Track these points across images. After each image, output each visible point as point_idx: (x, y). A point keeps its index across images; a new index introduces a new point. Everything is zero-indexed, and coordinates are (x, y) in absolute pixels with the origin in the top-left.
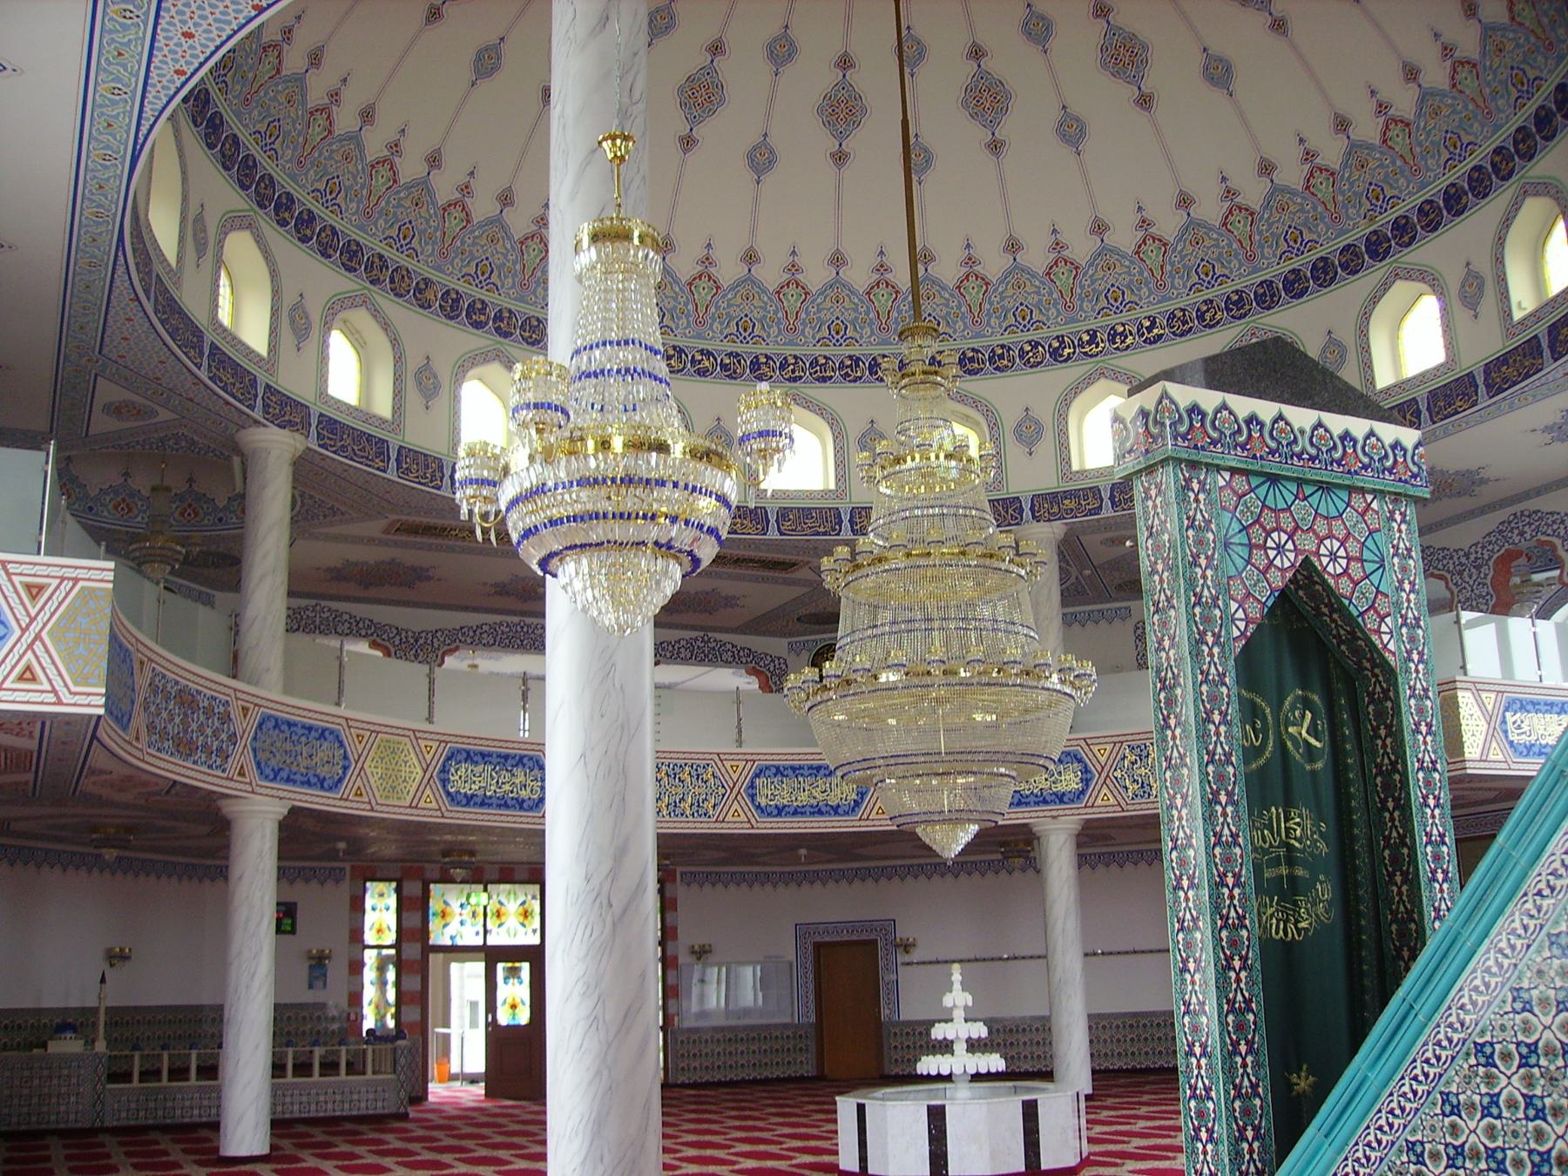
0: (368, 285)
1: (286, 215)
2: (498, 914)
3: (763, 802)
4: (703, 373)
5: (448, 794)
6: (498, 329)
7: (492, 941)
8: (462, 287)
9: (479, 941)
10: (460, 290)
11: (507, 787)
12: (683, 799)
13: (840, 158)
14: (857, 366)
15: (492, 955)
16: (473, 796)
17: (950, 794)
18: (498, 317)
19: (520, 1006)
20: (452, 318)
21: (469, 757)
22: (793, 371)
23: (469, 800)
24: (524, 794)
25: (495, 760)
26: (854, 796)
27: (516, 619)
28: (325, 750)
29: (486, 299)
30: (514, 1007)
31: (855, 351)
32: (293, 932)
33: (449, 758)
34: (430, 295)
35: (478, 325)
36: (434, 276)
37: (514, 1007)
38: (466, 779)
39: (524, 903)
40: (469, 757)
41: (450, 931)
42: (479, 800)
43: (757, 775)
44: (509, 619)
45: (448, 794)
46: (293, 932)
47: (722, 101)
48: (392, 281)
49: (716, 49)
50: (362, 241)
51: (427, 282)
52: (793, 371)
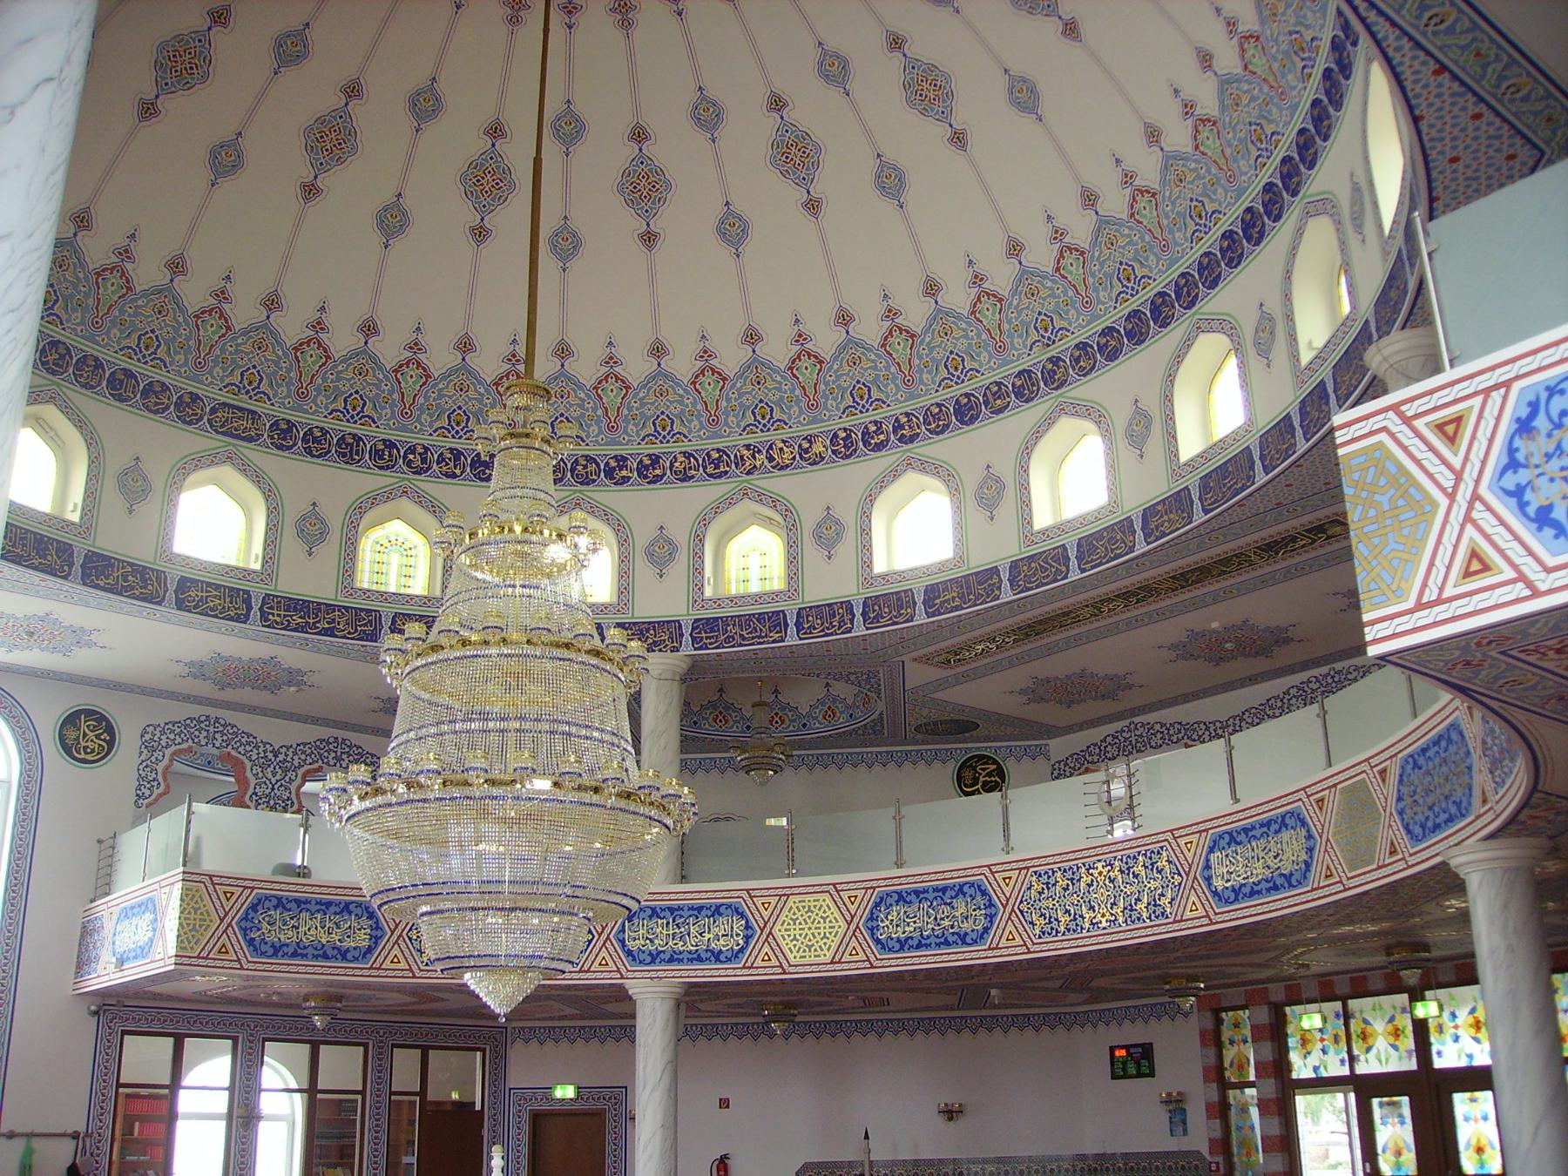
0: (746, 477)
1: (624, 473)
2: (1364, 1036)
3: (1218, 883)
4: (1113, 356)
5: (878, 941)
6: (902, 439)
7: (1361, 1069)
8: (847, 422)
9: (1345, 1071)
10: (846, 425)
11: (946, 923)
12: (1138, 900)
13: (1071, 29)
14: (1234, 241)
15: (1367, 1088)
16: (907, 939)
17: (501, 935)
18: (898, 426)
19: (1488, 1151)
20: (848, 457)
21: (901, 898)
22: (1188, 293)
23: (903, 944)
24: (966, 927)
25: (931, 896)
26: (1304, 857)
27: (1324, 670)
28: (722, 925)
29: (877, 418)
30: (1480, 1150)
31: (1223, 225)
32: (1152, 1074)
33: (877, 905)
34: (818, 448)
35: (879, 447)
36: (813, 429)
37: (1480, 1150)
38: (894, 923)
39: (1392, 1019)
40: (901, 898)
41: (1314, 1059)
42: (915, 942)
43: (1211, 850)
44: (1317, 672)
45: (878, 941)
46: (1152, 1074)
47: (948, 79)
48: (771, 459)
49: (896, 43)
50: (720, 446)
51: (810, 439)
52: (1188, 293)
